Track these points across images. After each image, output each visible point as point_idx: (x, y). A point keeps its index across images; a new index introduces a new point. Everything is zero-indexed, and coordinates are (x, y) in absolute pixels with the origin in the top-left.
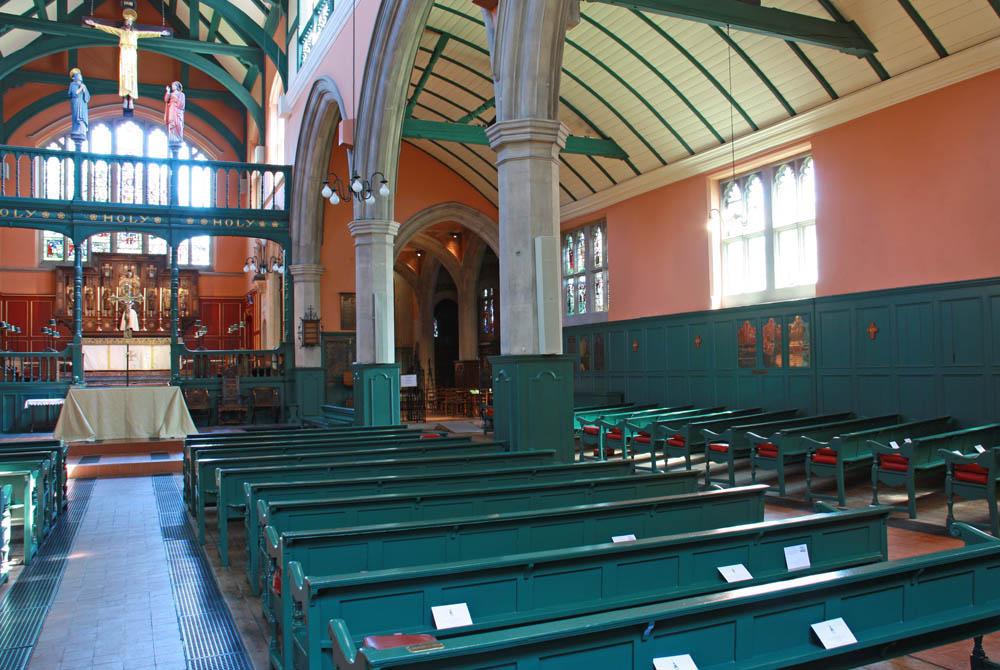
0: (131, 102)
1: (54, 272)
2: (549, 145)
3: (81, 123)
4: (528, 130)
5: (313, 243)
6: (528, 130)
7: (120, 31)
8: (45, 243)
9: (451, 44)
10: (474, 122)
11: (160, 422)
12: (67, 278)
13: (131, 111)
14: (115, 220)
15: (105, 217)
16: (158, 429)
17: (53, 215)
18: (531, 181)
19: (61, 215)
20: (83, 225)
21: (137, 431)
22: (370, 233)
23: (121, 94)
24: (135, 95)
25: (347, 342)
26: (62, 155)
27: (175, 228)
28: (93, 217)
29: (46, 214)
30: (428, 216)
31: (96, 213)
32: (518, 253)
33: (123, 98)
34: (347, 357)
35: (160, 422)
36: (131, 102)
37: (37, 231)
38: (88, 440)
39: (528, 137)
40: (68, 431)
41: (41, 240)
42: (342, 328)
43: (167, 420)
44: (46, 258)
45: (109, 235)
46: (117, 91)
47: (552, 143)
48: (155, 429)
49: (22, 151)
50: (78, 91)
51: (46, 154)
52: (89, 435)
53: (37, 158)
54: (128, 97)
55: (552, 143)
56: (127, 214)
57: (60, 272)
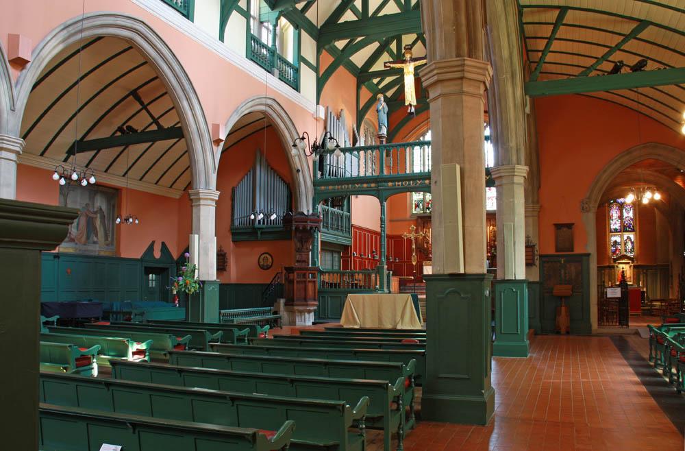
0: (413, 108)
1: (417, 220)
2: (460, 82)
3: (383, 126)
4: (435, 72)
5: (530, 187)
6: (435, 72)
7: (403, 65)
8: (414, 202)
9: (570, 17)
10: (593, 73)
11: (398, 318)
12: (424, 224)
13: (413, 113)
14: (402, 185)
15: (397, 183)
18: (442, 117)
19: (373, 185)
21: (384, 323)
22: (501, 177)
23: (407, 104)
24: (414, 103)
25: (560, 262)
26: (422, 144)
27: (381, 190)
28: (390, 184)
29: (365, 185)
30: (627, 157)
31: (391, 181)
32: (436, 182)
33: (408, 106)
34: (560, 273)
35: (398, 318)
36: (413, 108)
37: (408, 193)
39: (435, 78)
40: (347, 320)
41: (411, 200)
42: (557, 251)
43: (402, 317)
44: (414, 212)
45: (422, 193)
46: (405, 103)
47: (462, 78)
48: (395, 321)
49: (400, 146)
50: (381, 108)
51: (413, 145)
52: (355, 323)
53: (408, 149)
54: (410, 105)
55: (462, 78)
56: (409, 180)
57: (419, 219)
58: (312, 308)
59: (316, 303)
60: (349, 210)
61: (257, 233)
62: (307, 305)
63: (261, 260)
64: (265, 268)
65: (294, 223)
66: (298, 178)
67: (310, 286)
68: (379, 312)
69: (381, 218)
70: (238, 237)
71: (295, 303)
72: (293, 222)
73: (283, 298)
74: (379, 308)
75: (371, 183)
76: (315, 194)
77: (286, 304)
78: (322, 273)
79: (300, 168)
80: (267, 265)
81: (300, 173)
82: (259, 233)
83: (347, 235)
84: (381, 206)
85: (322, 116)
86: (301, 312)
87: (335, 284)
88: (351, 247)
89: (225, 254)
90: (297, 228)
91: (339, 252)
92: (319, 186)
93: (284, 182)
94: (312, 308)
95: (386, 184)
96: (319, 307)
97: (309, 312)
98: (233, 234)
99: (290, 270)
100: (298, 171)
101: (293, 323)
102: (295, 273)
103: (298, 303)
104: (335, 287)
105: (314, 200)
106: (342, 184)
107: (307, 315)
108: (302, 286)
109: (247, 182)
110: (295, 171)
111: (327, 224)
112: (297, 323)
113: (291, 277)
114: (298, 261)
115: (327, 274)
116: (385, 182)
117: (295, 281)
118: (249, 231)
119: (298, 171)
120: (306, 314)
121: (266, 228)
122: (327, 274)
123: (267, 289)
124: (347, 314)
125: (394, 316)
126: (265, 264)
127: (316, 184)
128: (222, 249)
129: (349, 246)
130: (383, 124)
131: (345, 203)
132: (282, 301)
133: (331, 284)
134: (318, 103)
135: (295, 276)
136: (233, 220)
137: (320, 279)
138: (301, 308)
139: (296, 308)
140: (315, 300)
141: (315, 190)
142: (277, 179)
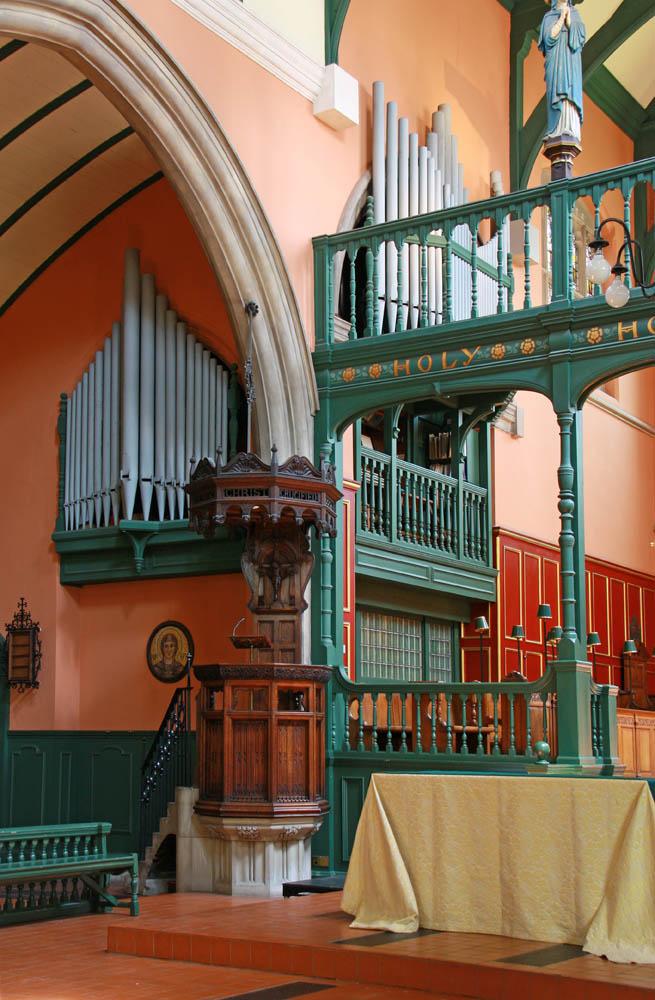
14: (643, 332)
15: (620, 328)
16: (586, 921)
17: (511, 348)
19: (528, 345)
20: (573, 359)
28: (594, 333)
29: (498, 349)
35: (593, 897)
38: (397, 927)
48: (578, 917)
52: (399, 910)
58: (292, 827)
59: (311, 806)
60: (483, 479)
61: (131, 551)
62: (270, 815)
63: (156, 649)
64: (169, 674)
65: (220, 496)
66: (250, 329)
67: (287, 742)
68: (506, 861)
69: (561, 473)
70: (80, 570)
71: (228, 804)
72: (219, 493)
73: (188, 784)
74: (504, 839)
75: (522, 336)
76: (322, 397)
77: (199, 810)
78: (354, 692)
79: (257, 300)
80: (174, 667)
81: (260, 317)
82: (139, 547)
83: (479, 564)
84: (561, 423)
85: (352, 111)
86: (252, 841)
87: (397, 735)
88: (494, 604)
89: (35, 628)
90: (234, 512)
91: (455, 625)
92: (333, 367)
93: (219, 362)
94: (292, 827)
95: (576, 336)
96: (322, 815)
97: (284, 841)
98: (65, 558)
99: (212, 678)
100: (251, 309)
101: (223, 886)
102: (228, 690)
103: (242, 805)
104: (397, 747)
105: (318, 417)
106: (414, 355)
107: (274, 854)
108: (253, 736)
109: (102, 367)
110: (238, 311)
111: (386, 515)
112: (239, 884)
113: (217, 707)
114: (240, 644)
115: (381, 696)
116: (572, 327)
117: (228, 720)
118: (111, 543)
119: (251, 309)
120: (271, 848)
121: (162, 531)
122: (367, 696)
123: (154, 748)
124: (369, 874)
125: (574, 887)
126: (169, 662)
127: (324, 360)
128: (27, 610)
129: (487, 602)
130: (564, 97)
131: (468, 448)
132: (187, 796)
133: (382, 734)
134: (331, 57)
135: (225, 700)
136: (61, 510)
137: (343, 712)
138: (250, 826)
139: (229, 824)
140: (308, 797)
141: (321, 383)
142: (197, 354)
